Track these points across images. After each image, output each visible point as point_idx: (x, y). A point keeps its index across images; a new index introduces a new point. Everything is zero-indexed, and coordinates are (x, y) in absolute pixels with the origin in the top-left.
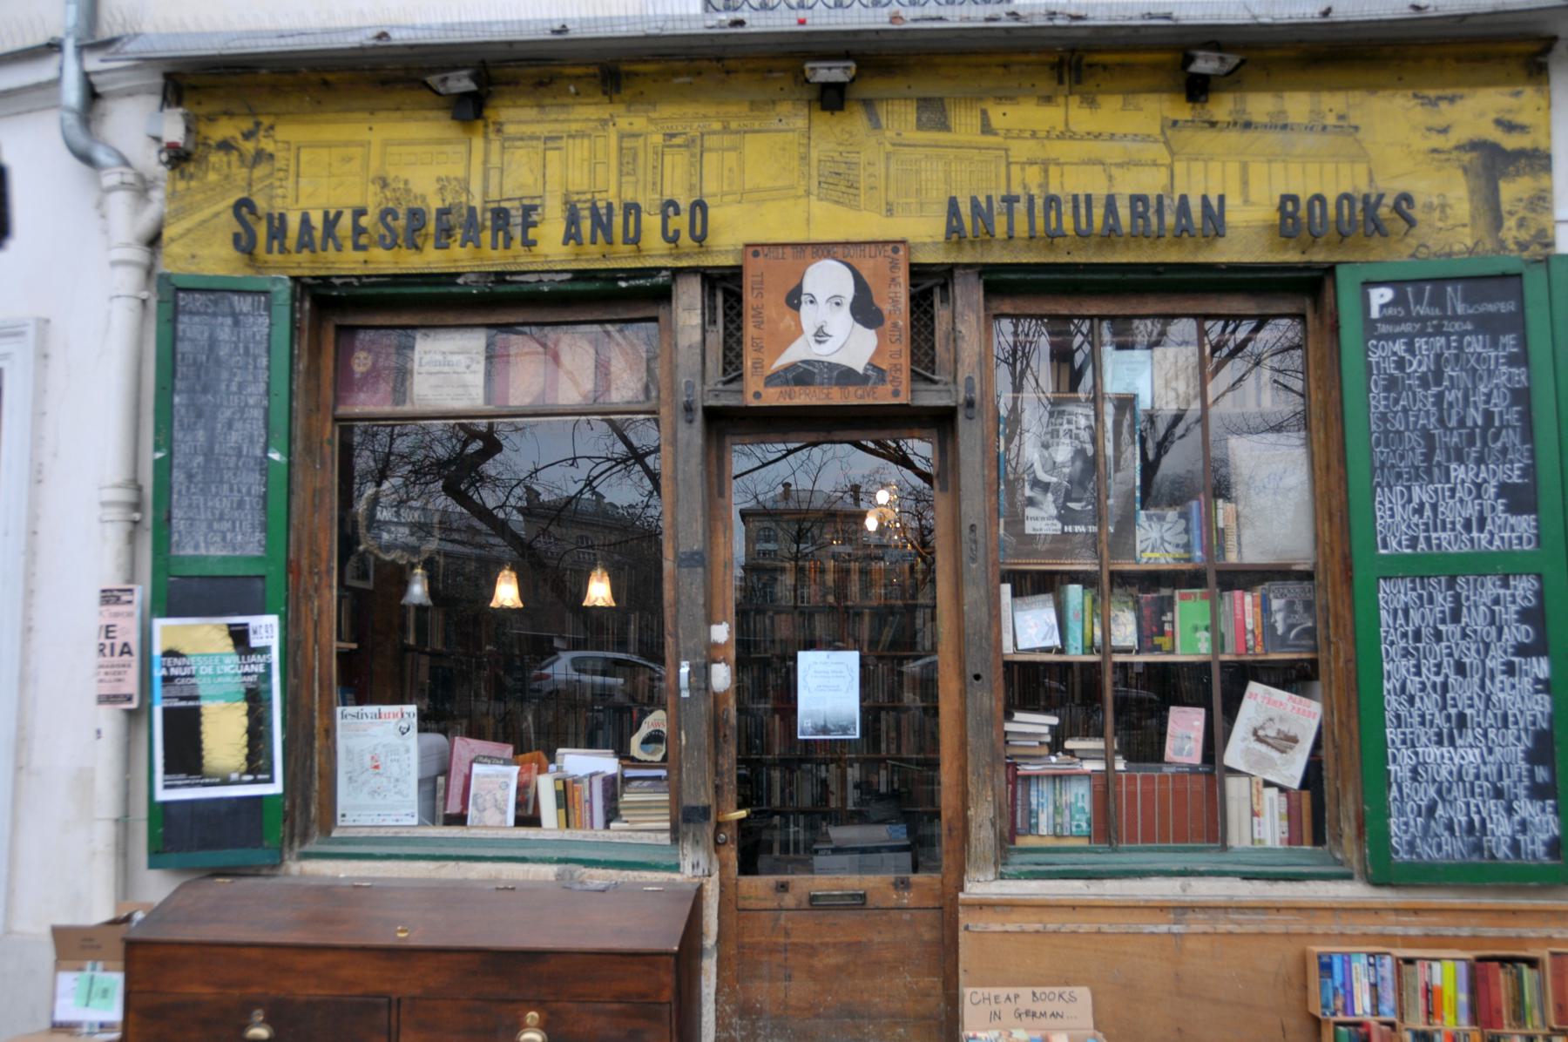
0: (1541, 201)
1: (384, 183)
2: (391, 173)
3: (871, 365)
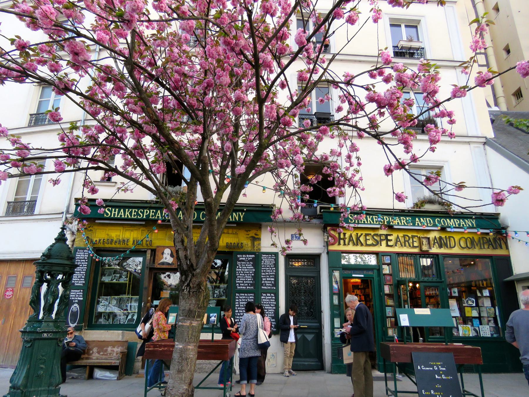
0: (259, 244)
1: (108, 235)
2: (109, 234)
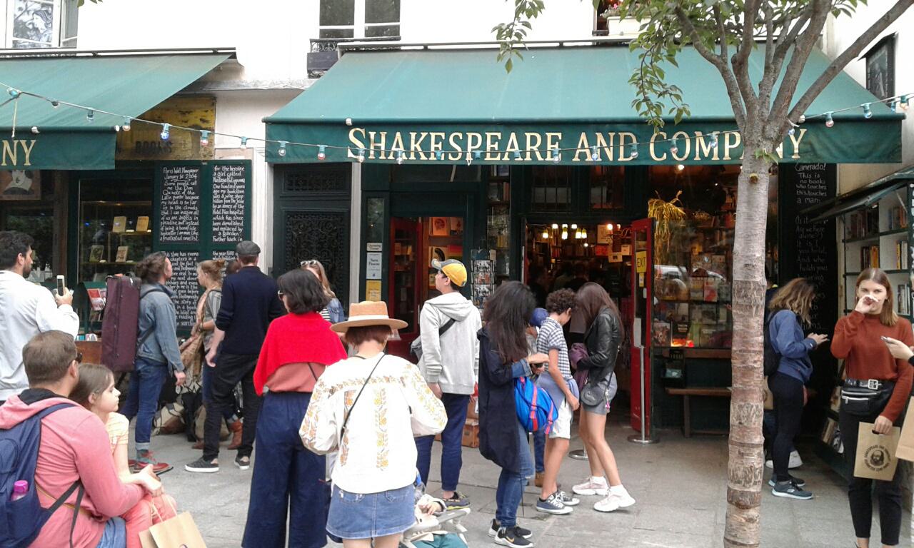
3: (30, 189)
